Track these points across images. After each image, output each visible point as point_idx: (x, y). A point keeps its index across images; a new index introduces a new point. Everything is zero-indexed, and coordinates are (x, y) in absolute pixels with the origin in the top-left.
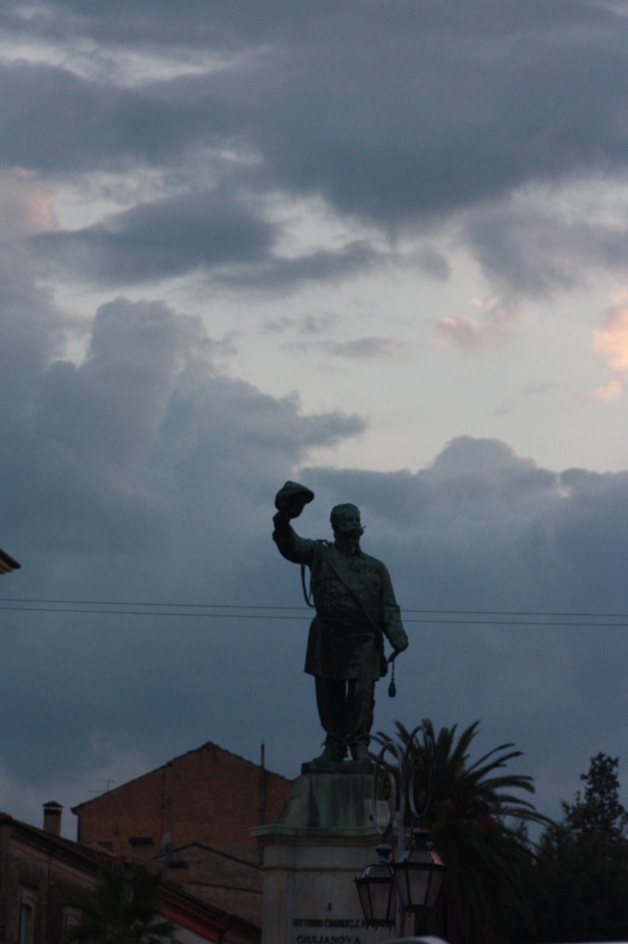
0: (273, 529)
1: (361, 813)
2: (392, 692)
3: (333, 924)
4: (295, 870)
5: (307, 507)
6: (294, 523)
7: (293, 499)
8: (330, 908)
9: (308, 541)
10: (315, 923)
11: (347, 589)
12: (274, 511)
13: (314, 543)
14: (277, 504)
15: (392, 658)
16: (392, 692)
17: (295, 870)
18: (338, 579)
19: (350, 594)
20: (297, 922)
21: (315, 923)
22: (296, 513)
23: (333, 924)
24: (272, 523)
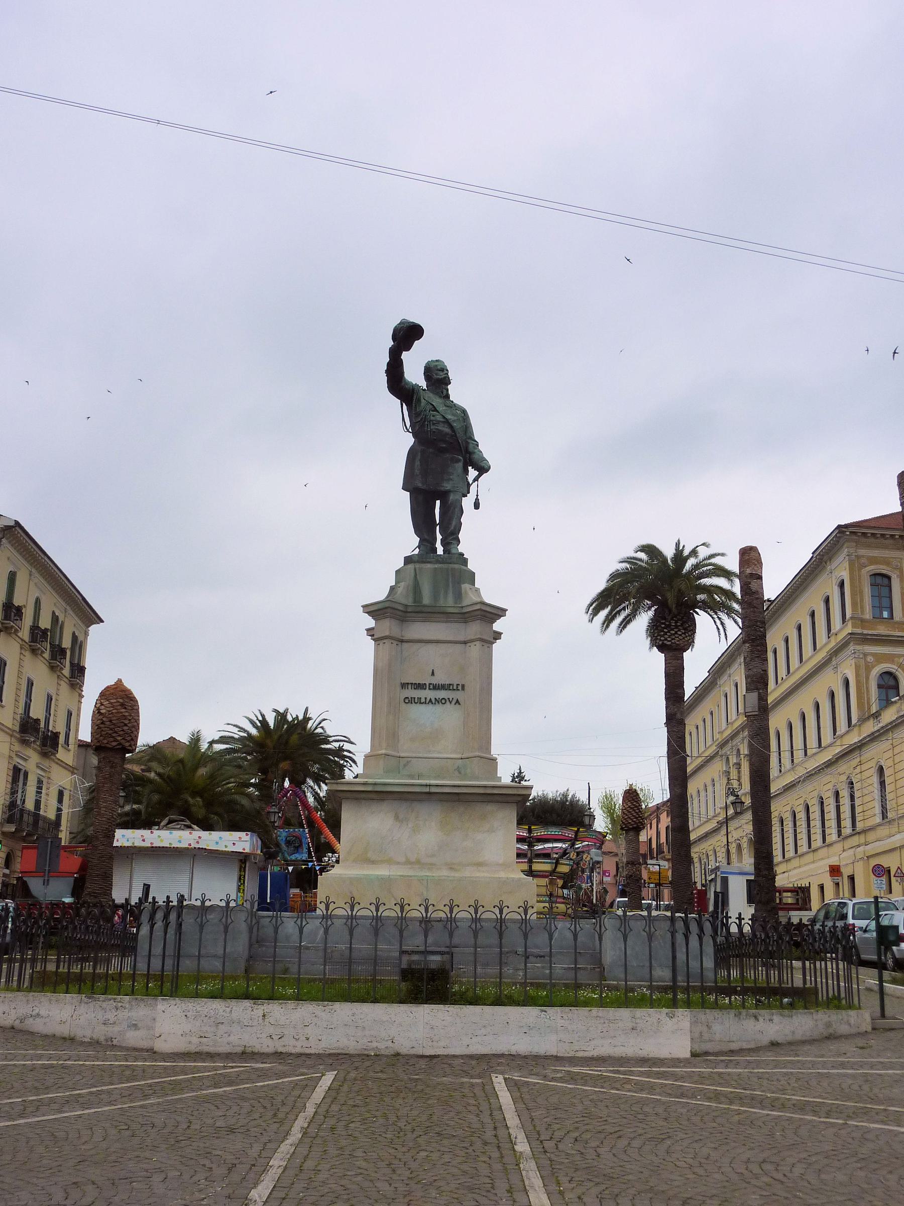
2: (477, 506)
3: (436, 687)
4: (402, 641)
6: (405, 356)
7: (407, 335)
8: (433, 674)
9: (408, 383)
10: (420, 686)
11: (444, 417)
13: (413, 385)
14: (394, 338)
16: (477, 506)
17: (402, 641)
18: (436, 410)
19: (447, 422)
20: (404, 686)
21: (420, 686)
23: (436, 687)
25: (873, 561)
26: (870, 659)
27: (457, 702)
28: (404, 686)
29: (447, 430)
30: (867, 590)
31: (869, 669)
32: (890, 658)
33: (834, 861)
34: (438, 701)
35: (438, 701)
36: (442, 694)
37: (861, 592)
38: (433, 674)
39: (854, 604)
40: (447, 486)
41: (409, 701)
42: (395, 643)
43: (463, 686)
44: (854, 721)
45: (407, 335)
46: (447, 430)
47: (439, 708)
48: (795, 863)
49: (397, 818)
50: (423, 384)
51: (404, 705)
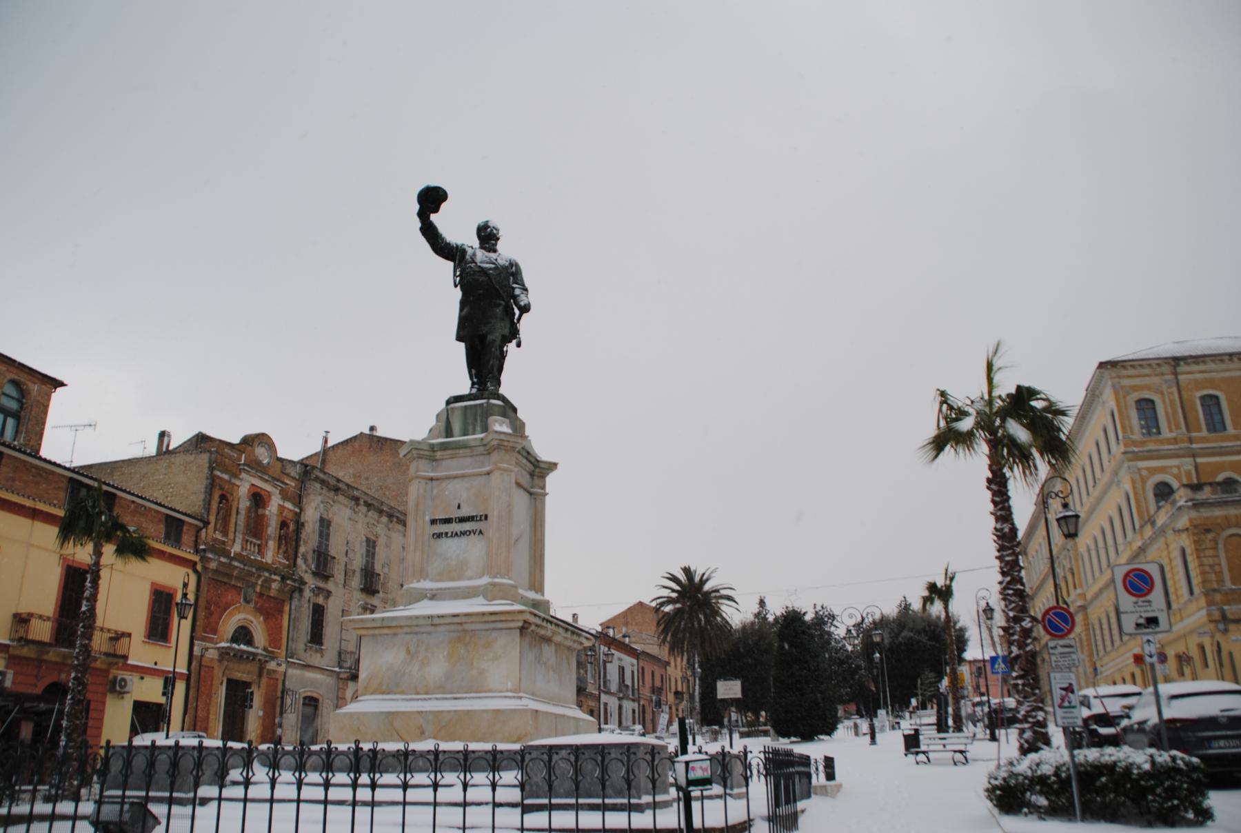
0: (419, 225)
1: (485, 429)
2: (519, 345)
3: (463, 520)
5: (444, 206)
7: (431, 199)
8: (459, 507)
10: (448, 521)
12: (417, 207)
15: (519, 319)
16: (519, 345)
20: (433, 522)
21: (448, 521)
22: (436, 210)
23: (463, 520)
24: (417, 219)
25: (1135, 388)
26: (1144, 473)
27: (481, 532)
28: (433, 522)
29: (483, 278)
30: (1134, 414)
31: (1144, 481)
32: (1162, 470)
33: (1137, 651)
34: (463, 533)
35: (463, 533)
36: (467, 526)
37: (1129, 418)
38: (459, 507)
39: (1123, 427)
40: (485, 329)
41: (439, 536)
42: (423, 482)
43: (486, 517)
44: (1137, 526)
45: (431, 199)
46: (483, 278)
47: (464, 539)
48: (1114, 654)
49: (408, 651)
50: (476, 243)
51: (432, 541)
